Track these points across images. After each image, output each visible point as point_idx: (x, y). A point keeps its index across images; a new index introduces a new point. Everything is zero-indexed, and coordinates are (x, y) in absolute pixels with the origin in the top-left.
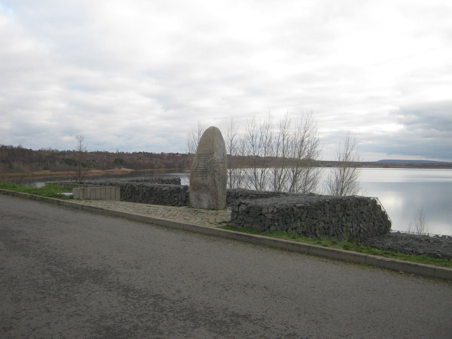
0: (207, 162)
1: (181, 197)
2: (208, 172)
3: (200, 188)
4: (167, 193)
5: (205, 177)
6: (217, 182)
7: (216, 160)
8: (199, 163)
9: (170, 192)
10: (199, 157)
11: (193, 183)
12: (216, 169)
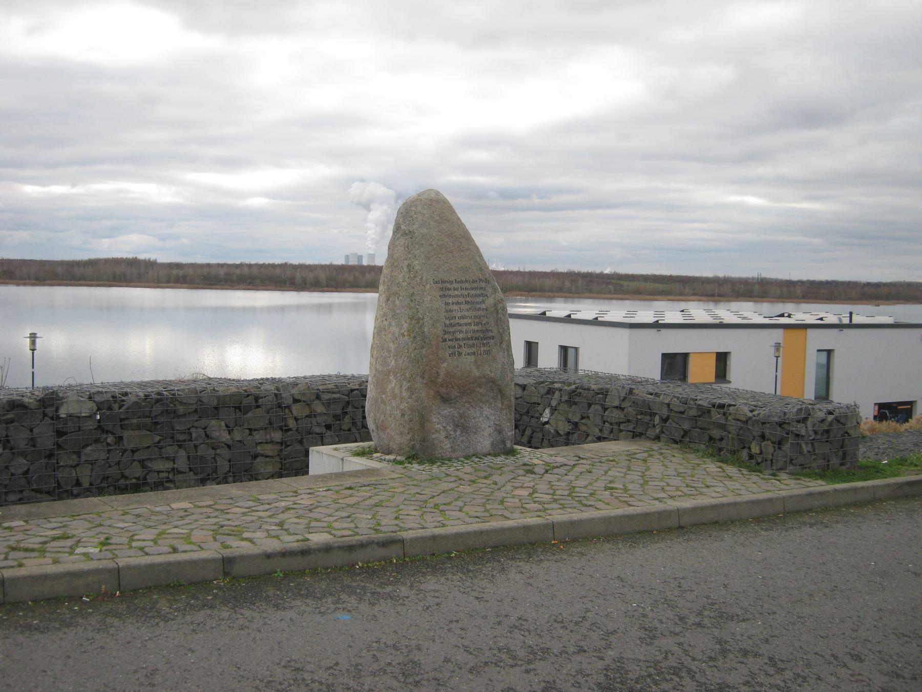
0: (483, 306)
2: (493, 338)
10: (442, 289)
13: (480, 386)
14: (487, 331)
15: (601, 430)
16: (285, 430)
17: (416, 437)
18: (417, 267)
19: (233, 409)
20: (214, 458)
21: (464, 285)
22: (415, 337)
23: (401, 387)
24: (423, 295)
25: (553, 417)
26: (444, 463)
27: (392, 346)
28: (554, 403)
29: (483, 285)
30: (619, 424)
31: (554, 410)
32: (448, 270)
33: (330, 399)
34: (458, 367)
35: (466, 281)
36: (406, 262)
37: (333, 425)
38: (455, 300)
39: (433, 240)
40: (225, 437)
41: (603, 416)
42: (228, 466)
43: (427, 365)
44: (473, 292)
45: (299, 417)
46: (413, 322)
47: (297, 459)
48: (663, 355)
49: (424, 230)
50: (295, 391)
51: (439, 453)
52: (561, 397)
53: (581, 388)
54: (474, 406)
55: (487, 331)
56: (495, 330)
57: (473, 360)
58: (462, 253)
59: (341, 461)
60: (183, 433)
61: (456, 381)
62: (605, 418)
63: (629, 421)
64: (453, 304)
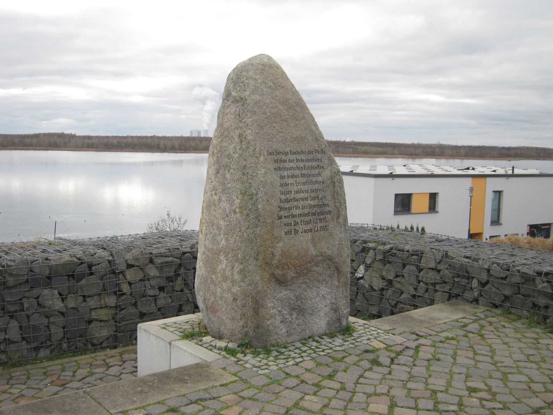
0: (320, 179)
2: (330, 212)
5: (322, 232)
10: (276, 161)
13: (317, 265)
14: (325, 205)
15: (415, 289)
16: (119, 294)
17: (250, 324)
18: (250, 137)
19: (66, 277)
20: (48, 326)
21: (299, 157)
22: (248, 215)
23: (233, 268)
24: (257, 168)
25: (368, 273)
26: (282, 353)
27: (222, 223)
28: (368, 261)
29: (319, 156)
30: (434, 284)
31: (368, 267)
32: (282, 140)
33: (163, 263)
34: (294, 246)
35: (302, 152)
36: (237, 132)
37: (166, 287)
38: (290, 173)
39: (267, 108)
40: (59, 305)
41: (417, 276)
42: (63, 333)
43: (261, 246)
44: (309, 164)
45: (133, 282)
46: (245, 198)
47: (131, 321)
48: (397, 195)
49: (257, 97)
50: (129, 256)
51: (274, 339)
52: (375, 256)
53: (395, 249)
54: (311, 286)
55: (325, 205)
56: (331, 203)
57: (310, 238)
59: (168, 346)
60: (13, 303)
61: (292, 261)
62: (420, 279)
63: (445, 282)
64: (288, 177)
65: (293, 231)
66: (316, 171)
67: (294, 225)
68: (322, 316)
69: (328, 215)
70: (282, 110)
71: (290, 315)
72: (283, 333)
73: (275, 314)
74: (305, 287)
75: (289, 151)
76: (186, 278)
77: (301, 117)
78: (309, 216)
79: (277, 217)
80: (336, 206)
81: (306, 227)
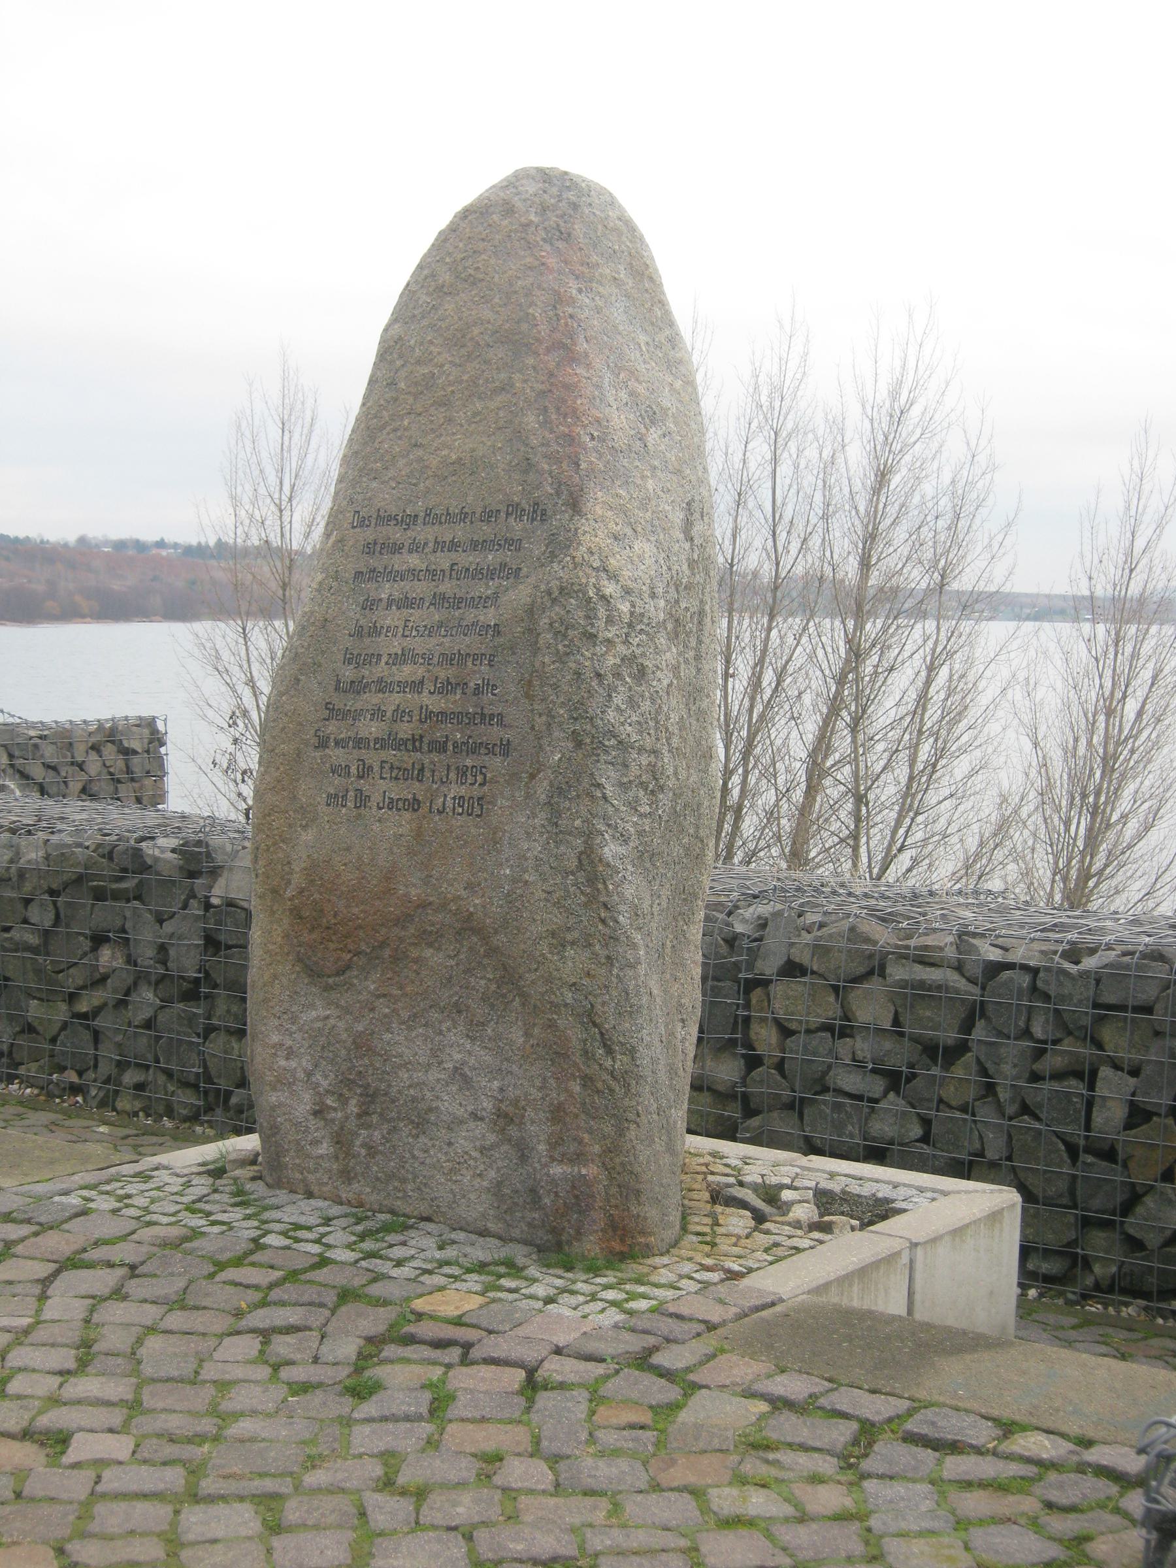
0: (489, 616)
1: (163, 948)
2: (506, 748)
3: (395, 959)
4: (27, 902)
6: (629, 891)
7: (610, 589)
8: (375, 631)
9: (52, 893)
10: (370, 548)
11: (297, 879)
12: (611, 715)
14: (485, 718)
35: (464, 516)
55: (485, 718)
58: (479, 406)
65: (351, 794)
66: (488, 587)
67: (360, 777)
68: (466, 1153)
69: (499, 759)
70: (442, 366)
71: (339, 1100)
72: (321, 1157)
73: (295, 1079)
74: (387, 1010)
75: (422, 514)
76: (988, 1065)
77: (497, 384)
78: (415, 749)
79: (314, 741)
80: (533, 728)
81: (396, 791)
